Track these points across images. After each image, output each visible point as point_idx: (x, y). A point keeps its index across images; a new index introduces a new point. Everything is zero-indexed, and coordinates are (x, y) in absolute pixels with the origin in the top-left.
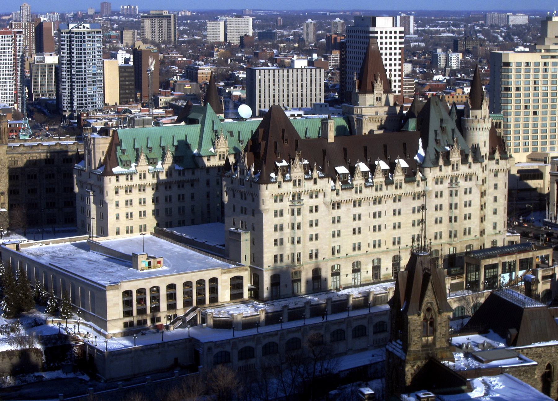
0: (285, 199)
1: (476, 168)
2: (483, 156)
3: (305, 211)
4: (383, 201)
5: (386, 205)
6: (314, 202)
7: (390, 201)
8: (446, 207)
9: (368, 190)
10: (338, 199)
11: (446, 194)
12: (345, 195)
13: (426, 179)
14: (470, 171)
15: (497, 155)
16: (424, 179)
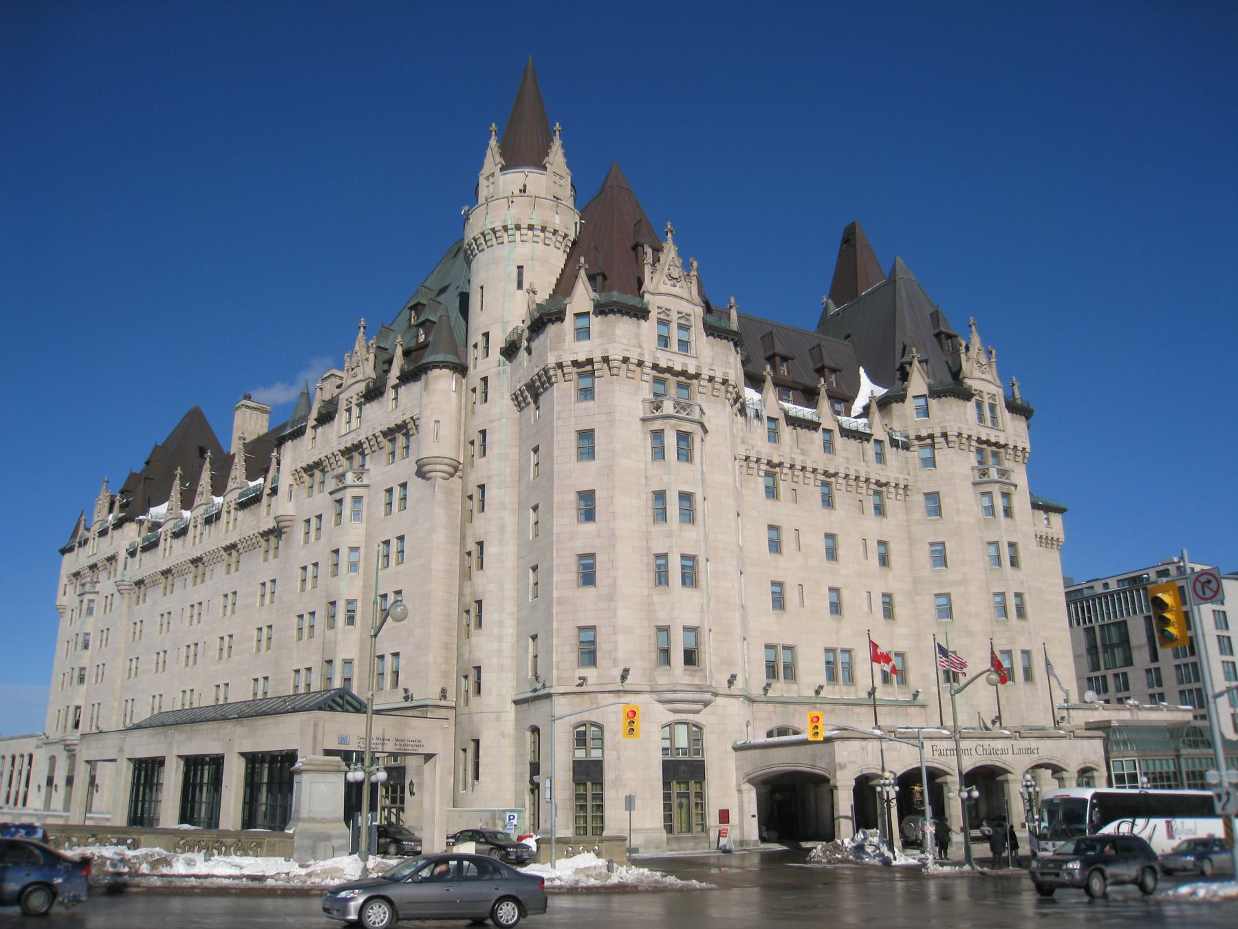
12: (151, 564)
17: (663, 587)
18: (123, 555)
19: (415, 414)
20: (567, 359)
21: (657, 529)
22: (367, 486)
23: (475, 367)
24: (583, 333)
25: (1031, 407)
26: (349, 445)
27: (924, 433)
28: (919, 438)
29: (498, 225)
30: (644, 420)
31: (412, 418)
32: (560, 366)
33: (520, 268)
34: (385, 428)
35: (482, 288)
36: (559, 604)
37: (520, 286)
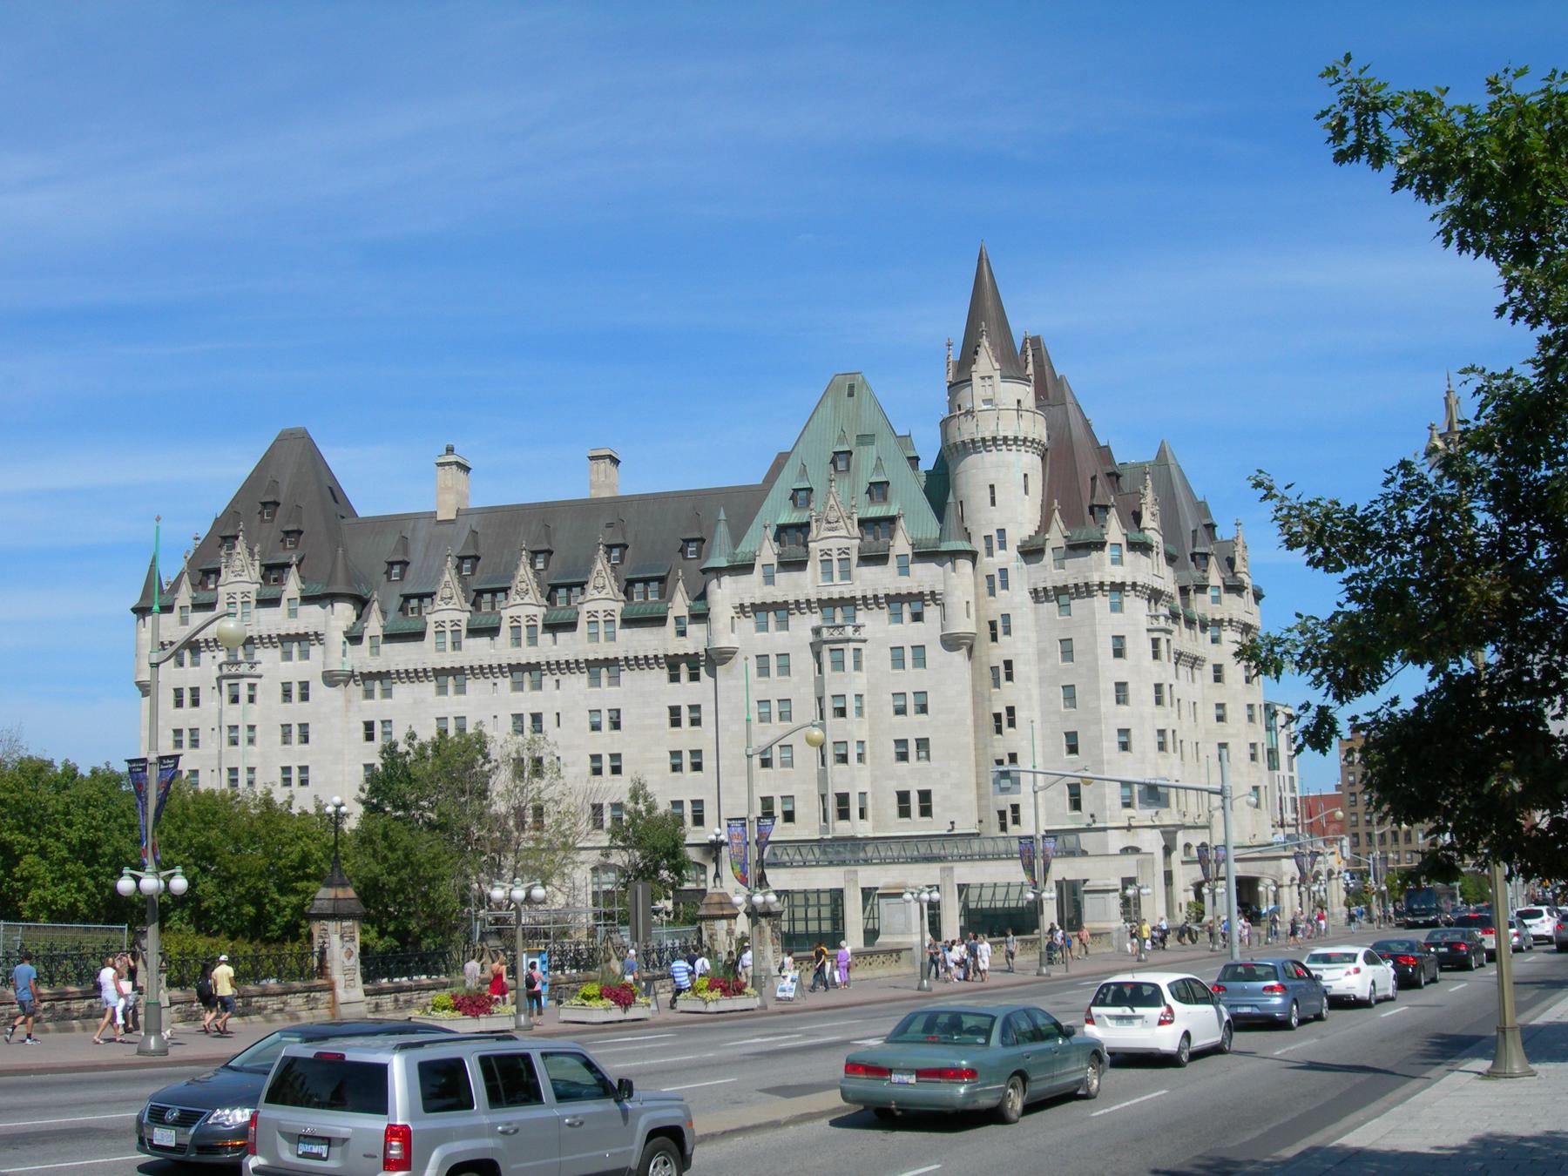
0: (205, 656)
1: (925, 576)
2: (988, 538)
3: (269, 692)
4: (548, 681)
5: (558, 692)
6: (296, 669)
7: (577, 683)
8: (804, 710)
9: (484, 641)
10: (375, 665)
11: (803, 662)
13: (709, 609)
14: (905, 585)
15: (1056, 537)
16: (701, 617)
17: (1163, 753)
18: (337, 637)
19: (938, 588)
20: (1107, 580)
21: (1159, 710)
22: (865, 641)
23: (990, 553)
24: (1118, 561)
25: (1264, 593)
26: (836, 596)
27: (1217, 617)
28: (1213, 619)
29: (1011, 435)
30: (1148, 630)
31: (933, 593)
32: (1101, 585)
33: (1026, 475)
34: (893, 592)
35: (992, 487)
36: (1109, 763)
37: (1026, 492)
